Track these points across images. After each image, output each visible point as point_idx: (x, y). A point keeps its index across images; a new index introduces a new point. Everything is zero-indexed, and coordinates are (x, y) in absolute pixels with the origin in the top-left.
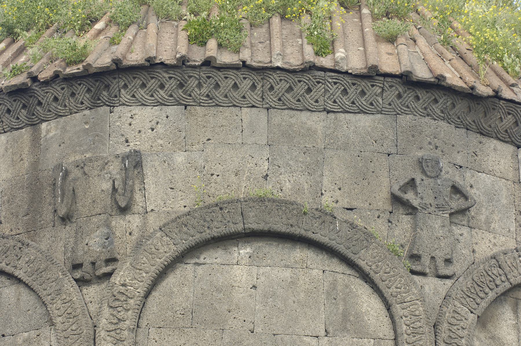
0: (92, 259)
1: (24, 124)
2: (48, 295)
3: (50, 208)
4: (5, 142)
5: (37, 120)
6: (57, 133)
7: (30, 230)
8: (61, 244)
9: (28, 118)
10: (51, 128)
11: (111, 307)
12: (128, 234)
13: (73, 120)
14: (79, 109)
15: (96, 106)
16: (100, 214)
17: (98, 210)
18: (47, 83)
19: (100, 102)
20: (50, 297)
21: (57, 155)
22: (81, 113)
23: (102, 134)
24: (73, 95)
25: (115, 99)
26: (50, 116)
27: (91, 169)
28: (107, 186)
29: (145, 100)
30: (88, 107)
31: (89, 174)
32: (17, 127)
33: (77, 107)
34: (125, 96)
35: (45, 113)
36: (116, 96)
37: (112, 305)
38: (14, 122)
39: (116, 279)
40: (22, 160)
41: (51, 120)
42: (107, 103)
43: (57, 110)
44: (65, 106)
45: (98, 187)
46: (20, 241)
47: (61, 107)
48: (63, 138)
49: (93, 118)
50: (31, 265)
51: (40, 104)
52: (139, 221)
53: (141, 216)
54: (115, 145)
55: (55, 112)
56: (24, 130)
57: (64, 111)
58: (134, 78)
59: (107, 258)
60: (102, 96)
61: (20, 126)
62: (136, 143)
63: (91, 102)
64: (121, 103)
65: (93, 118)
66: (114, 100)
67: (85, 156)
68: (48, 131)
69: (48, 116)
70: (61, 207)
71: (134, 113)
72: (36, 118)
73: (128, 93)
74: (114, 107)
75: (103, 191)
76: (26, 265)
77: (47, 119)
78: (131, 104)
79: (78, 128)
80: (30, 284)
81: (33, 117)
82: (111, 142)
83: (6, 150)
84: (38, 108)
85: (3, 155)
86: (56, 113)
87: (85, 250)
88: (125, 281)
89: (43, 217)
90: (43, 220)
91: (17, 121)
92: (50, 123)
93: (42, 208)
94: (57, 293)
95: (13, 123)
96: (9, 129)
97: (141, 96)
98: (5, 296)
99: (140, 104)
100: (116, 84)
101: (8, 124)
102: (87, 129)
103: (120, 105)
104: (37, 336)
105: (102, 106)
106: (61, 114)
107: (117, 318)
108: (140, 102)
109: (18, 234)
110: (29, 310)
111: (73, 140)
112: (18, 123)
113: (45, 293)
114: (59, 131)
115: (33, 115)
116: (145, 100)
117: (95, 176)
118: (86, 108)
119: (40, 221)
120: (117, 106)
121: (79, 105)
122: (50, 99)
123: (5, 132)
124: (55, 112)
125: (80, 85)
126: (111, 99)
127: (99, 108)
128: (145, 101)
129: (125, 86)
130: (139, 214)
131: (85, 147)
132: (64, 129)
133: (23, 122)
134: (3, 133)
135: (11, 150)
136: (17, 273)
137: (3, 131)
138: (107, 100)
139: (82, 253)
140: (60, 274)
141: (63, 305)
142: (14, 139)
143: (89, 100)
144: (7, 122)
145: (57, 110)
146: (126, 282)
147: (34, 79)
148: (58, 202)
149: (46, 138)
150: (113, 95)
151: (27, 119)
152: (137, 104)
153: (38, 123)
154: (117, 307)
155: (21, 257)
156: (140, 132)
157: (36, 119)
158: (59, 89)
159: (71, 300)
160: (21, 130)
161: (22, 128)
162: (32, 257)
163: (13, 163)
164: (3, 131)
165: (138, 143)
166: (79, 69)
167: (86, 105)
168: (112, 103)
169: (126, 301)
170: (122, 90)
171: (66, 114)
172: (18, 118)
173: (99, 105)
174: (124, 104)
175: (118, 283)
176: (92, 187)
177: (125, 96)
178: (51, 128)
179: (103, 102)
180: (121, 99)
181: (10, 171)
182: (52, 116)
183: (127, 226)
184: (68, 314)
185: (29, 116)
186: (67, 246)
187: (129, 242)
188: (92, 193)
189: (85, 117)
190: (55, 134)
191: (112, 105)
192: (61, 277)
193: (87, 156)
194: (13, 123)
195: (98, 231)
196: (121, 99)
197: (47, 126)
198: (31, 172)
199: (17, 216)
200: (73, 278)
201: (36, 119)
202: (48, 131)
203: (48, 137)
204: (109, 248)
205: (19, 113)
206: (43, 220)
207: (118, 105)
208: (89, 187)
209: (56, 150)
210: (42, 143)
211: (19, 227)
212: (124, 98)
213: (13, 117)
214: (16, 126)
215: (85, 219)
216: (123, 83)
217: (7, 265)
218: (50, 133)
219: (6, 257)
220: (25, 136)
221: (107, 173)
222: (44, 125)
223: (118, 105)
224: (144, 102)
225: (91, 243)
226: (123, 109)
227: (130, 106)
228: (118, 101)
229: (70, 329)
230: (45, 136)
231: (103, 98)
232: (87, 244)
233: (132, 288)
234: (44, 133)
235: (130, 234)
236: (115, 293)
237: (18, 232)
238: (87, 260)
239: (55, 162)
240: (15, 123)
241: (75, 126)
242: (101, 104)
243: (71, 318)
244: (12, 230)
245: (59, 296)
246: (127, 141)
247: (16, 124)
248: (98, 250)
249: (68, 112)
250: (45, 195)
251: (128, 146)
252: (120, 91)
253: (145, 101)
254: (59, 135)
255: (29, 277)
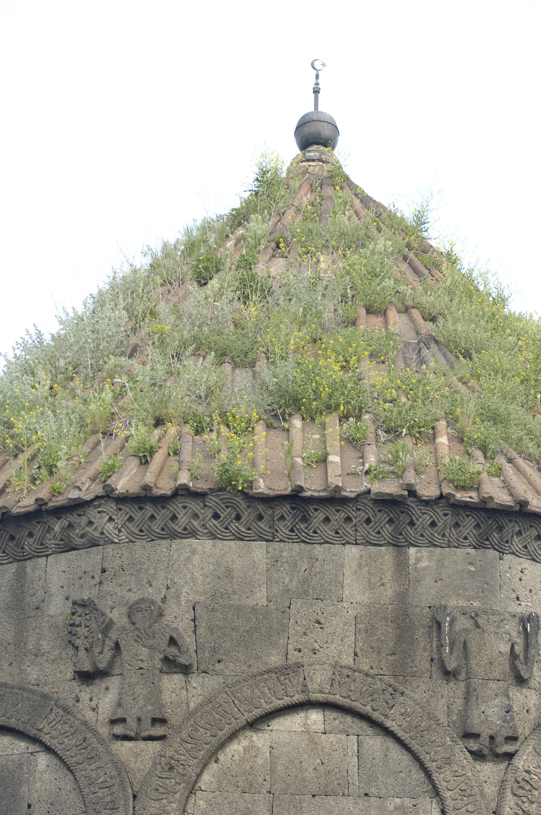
0: (491, 732)
1: (386, 542)
2: (433, 761)
3: (426, 654)
4: (357, 556)
5: (403, 542)
6: (431, 565)
7: (398, 674)
8: (443, 702)
9: (393, 536)
10: (422, 556)
11: (515, 795)
12: (525, 711)
13: (453, 555)
14: (460, 544)
15: (483, 547)
16: (499, 680)
17: (496, 675)
18: (427, 503)
19: (487, 542)
20: (435, 763)
21: (432, 592)
22: (463, 550)
23: (492, 583)
24: (457, 525)
25: (506, 545)
26: (422, 542)
27: (486, 622)
28: (505, 648)
29: (537, 554)
30: (473, 545)
31: (484, 628)
32: (376, 542)
33: (458, 540)
34: (517, 544)
35: (417, 536)
36: (507, 542)
37: (516, 793)
38: (373, 536)
39: (520, 762)
40: (383, 585)
41: (422, 547)
42: (496, 547)
43: (433, 537)
44: (444, 535)
45: (495, 647)
46: (390, 686)
47: (438, 535)
48: (440, 574)
49: (480, 560)
50: (408, 719)
51: (412, 524)
52: (536, 698)
53: (538, 693)
54: (507, 600)
55: (430, 539)
56: (384, 548)
57: (441, 541)
58: (531, 526)
59: (510, 735)
60: (493, 537)
61: (380, 543)
62: (528, 604)
63: (477, 540)
64: (511, 551)
65: (480, 560)
66: (504, 545)
67: (472, 604)
68: (418, 560)
69: (420, 542)
70: (450, 659)
71: (524, 566)
72: (402, 539)
73: (521, 542)
74: (503, 553)
75: (500, 652)
76: (402, 718)
77: (417, 544)
78: (521, 555)
79: (459, 567)
80: (407, 742)
81: (400, 537)
82: (502, 595)
83: (360, 566)
84: (408, 528)
85: (356, 572)
86: (431, 540)
87: (482, 719)
88: (529, 767)
89: (415, 663)
90: (416, 667)
91: (377, 535)
92: (421, 550)
93: (414, 651)
94: (446, 762)
95: (371, 537)
96: (364, 541)
97: (533, 550)
98: (368, 747)
99: (530, 557)
100: (511, 528)
101: (365, 536)
102: (474, 572)
103: (510, 553)
104: (413, 806)
105: (489, 548)
106: (436, 543)
107: (522, 809)
108: (531, 555)
109: (381, 675)
110: (401, 772)
111: (454, 580)
112: (378, 538)
113: (428, 757)
114: (433, 564)
115: (401, 534)
116: (537, 554)
117: (491, 633)
118: (470, 546)
119: (412, 667)
120: (507, 554)
121: (462, 540)
122: (427, 522)
123: (356, 544)
124: (430, 539)
125: (468, 516)
126: (502, 543)
127: (487, 550)
128: (536, 556)
129: (519, 533)
130: (535, 689)
131: (472, 593)
132: (440, 562)
133: (385, 539)
134: (354, 544)
135: (367, 569)
136: (388, 723)
137: (354, 542)
138: (497, 543)
139: (478, 721)
140: (448, 739)
141: (455, 778)
142: (370, 557)
143: (475, 537)
144: (363, 533)
145: (433, 537)
146: (529, 769)
147: (412, 493)
148: (446, 652)
149: (416, 568)
150: (504, 540)
151: (392, 537)
152: (528, 557)
153: (404, 546)
154: (521, 796)
155: (394, 705)
156: (531, 591)
157: (404, 540)
158: (441, 514)
159: (466, 774)
160: (380, 548)
161: (381, 545)
162: (409, 710)
163: (371, 586)
164: (354, 542)
165: (529, 604)
166: (471, 497)
167: (470, 542)
168: (502, 549)
169: (530, 791)
170: (515, 537)
171: (444, 545)
172: (379, 533)
173: (486, 546)
174: (513, 553)
175: (521, 768)
176: (487, 645)
177: (517, 544)
178: (422, 556)
179: (491, 544)
180: (512, 546)
181: (367, 594)
182: (424, 542)
183: (524, 701)
184: (461, 790)
185: (394, 535)
186: (452, 707)
187: (527, 721)
188: (488, 652)
189: (467, 555)
190: (429, 566)
191: (501, 550)
192: (449, 743)
193: (475, 604)
194: (371, 537)
195: (497, 700)
196: (512, 546)
197: (417, 553)
198: (396, 603)
199: (379, 653)
200: (466, 748)
201: (404, 540)
202: (418, 560)
203: (419, 566)
204: (511, 724)
205: (382, 528)
206: (416, 667)
207: (507, 552)
208: (485, 644)
209: (431, 585)
210: (411, 572)
211: (383, 667)
212: (516, 546)
213: (373, 529)
214: (374, 540)
215: (480, 681)
216: (518, 529)
217: (374, 710)
218: (421, 562)
219: (372, 700)
220: (386, 557)
221: (505, 633)
222: (412, 551)
223: (507, 552)
224: (535, 557)
225: (489, 712)
226: (513, 559)
227: (520, 557)
228: (508, 548)
229: (464, 809)
230: (414, 564)
231: (492, 539)
232: (483, 713)
233: (536, 778)
234: (412, 561)
235: (527, 711)
236: (519, 779)
237: (381, 672)
238: (485, 733)
239: (430, 599)
240: (373, 536)
241: (456, 563)
242: (489, 546)
243: (466, 796)
244: (372, 668)
245: (448, 766)
246: (518, 599)
247: (375, 538)
248: (498, 723)
249: (445, 544)
250: (417, 637)
251: (520, 604)
252: (512, 536)
253: (536, 556)
254: (434, 568)
255: (405, 732)
